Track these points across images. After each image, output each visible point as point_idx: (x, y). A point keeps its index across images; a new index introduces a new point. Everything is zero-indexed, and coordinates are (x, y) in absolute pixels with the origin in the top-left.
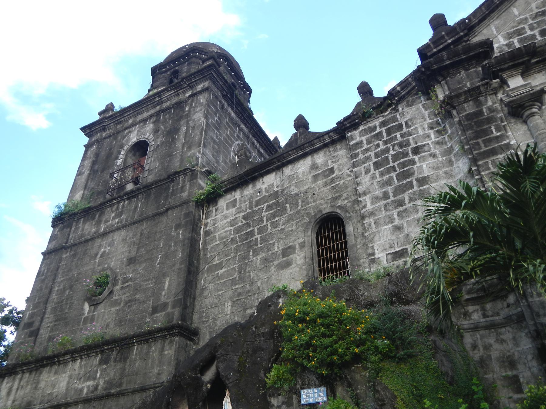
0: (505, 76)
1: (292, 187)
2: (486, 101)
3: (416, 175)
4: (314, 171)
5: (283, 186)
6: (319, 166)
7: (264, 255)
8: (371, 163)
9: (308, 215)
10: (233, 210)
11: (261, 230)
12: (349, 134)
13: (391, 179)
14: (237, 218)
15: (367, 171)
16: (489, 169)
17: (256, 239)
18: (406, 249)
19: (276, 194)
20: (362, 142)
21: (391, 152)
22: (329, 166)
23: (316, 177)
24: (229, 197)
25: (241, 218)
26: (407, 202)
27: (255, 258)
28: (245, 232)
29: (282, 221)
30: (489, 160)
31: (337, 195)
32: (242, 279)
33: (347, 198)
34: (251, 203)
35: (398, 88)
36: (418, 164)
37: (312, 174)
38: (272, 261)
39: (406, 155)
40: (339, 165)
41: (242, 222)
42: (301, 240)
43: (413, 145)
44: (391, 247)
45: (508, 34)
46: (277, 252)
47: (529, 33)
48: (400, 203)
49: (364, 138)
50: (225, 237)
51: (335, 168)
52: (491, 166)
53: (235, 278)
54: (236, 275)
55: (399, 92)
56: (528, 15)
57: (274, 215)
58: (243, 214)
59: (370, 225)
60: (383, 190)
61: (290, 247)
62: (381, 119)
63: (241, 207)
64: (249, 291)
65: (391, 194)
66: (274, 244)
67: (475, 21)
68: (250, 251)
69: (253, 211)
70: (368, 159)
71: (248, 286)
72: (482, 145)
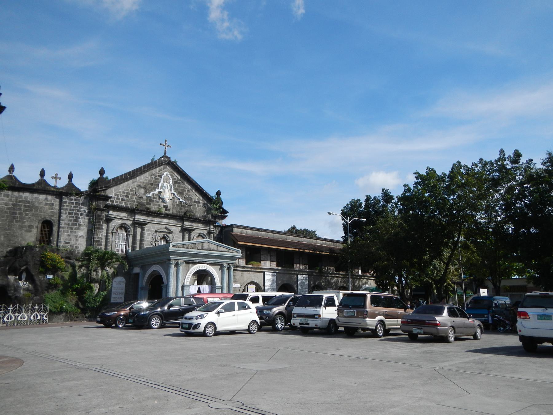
0: (110, 209)
1: (36, 203)
2: (103, 213)
3: (79, 222)
4: (46, 201)
5: (32, 200)
6: (49, 200)
7: (20, 224)
8: (68, 211)
9: (41, 217)
10: (5, 198)
11: (20, 214)
12: (64, 197)
13: (72, 220)
14: (8, 203)
15: (66, 214)
16: (96, 232)
17: (18, 216)
18: (69, 242)
19: (29, 202)
20: (67, 202)
21: (75, 211)
22: (52, 202)
23: (46, 204)
24: (6, 192)
25: (11, 204)
26: (74, 229)
27: (16, 224)
28: (12, 211)
29: (30, 215)
30: (97, 230)
31: (53, 215)
32: (9, 229)
33: (56, 218)
34: (16, 200)
35: (84, 192)
36: (80, 219)
37: (45, 202)
38: (24, 228)
39: (78, 215)
40: (56, 204)
41: (11, 206)
42: (37, 225)
43: (81, 213)
44: (66, 240)
45: (116, 194)
46: (26, 225)
47: (119, 197)
48: (72, 228)
49: (68, 201)
50: (2, 209)
51: (54, 204)
52: (97, 232)
53: (6, 228)
54: (6, 227)
55: (84, 193)
56: (122, 191)
57: (27, 210)
58: (12, 203)
59: (61, 231)
60: (68, 222)
61: (32, 226)
62: (75, 198)
63: (11, 199)
64: (12, 235)
65: (70, 225)
66: (25, 222)
67: (112, 186)
68: (14, 220)
69: (17, 204)
70: (67, 209)
71: (12, 233)
72: (98, 226)
